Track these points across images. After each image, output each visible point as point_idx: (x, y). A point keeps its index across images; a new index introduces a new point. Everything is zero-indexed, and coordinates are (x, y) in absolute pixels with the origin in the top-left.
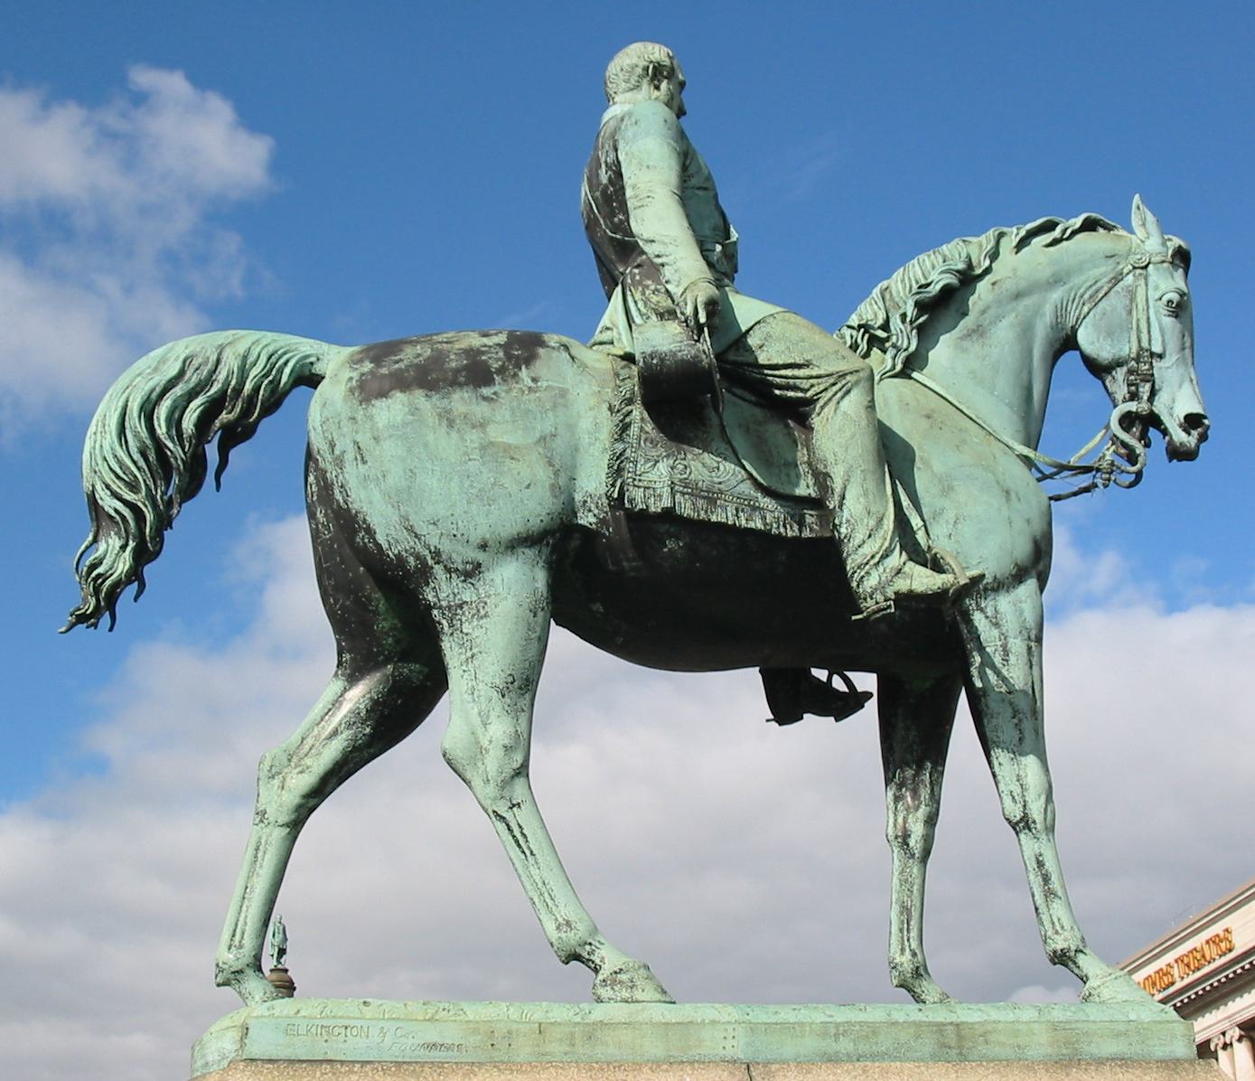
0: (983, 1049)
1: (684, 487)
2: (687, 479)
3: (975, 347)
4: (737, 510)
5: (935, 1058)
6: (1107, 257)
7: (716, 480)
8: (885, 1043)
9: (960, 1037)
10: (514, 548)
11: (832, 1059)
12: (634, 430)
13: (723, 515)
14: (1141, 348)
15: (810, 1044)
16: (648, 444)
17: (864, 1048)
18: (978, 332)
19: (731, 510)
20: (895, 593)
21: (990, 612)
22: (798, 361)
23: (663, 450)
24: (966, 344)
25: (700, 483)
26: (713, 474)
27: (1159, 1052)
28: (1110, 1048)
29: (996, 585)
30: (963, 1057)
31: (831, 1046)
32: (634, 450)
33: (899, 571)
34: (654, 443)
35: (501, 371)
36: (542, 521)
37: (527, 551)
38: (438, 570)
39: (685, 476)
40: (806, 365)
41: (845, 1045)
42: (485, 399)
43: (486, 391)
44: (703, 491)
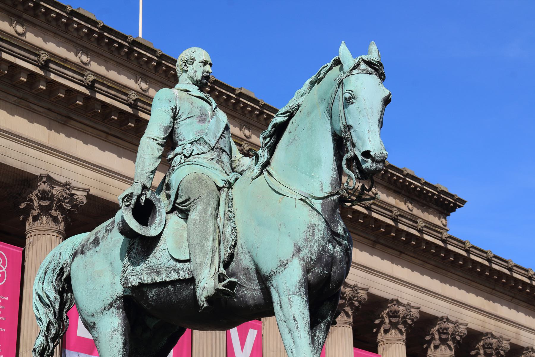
1: (148, 270)
2: (149, 267)
4: (168, 274)
6: (334, 80)
7: (159, 263)
10: (102, 313)
12: (134, 250)
13: (165, 277)
14: (344, 126)
16: (138, 255)
20: (205, 298)
21: (274, 285)
23: (142, 256)
25: (153, 267)
26: (159, 261)
29: (273, 273)
32: (132, 260)
34: (139, 254)
36: (108, 299)
37: (107, 312)
39: (148, 266)
43: (97, 249)
44: (154, 270)
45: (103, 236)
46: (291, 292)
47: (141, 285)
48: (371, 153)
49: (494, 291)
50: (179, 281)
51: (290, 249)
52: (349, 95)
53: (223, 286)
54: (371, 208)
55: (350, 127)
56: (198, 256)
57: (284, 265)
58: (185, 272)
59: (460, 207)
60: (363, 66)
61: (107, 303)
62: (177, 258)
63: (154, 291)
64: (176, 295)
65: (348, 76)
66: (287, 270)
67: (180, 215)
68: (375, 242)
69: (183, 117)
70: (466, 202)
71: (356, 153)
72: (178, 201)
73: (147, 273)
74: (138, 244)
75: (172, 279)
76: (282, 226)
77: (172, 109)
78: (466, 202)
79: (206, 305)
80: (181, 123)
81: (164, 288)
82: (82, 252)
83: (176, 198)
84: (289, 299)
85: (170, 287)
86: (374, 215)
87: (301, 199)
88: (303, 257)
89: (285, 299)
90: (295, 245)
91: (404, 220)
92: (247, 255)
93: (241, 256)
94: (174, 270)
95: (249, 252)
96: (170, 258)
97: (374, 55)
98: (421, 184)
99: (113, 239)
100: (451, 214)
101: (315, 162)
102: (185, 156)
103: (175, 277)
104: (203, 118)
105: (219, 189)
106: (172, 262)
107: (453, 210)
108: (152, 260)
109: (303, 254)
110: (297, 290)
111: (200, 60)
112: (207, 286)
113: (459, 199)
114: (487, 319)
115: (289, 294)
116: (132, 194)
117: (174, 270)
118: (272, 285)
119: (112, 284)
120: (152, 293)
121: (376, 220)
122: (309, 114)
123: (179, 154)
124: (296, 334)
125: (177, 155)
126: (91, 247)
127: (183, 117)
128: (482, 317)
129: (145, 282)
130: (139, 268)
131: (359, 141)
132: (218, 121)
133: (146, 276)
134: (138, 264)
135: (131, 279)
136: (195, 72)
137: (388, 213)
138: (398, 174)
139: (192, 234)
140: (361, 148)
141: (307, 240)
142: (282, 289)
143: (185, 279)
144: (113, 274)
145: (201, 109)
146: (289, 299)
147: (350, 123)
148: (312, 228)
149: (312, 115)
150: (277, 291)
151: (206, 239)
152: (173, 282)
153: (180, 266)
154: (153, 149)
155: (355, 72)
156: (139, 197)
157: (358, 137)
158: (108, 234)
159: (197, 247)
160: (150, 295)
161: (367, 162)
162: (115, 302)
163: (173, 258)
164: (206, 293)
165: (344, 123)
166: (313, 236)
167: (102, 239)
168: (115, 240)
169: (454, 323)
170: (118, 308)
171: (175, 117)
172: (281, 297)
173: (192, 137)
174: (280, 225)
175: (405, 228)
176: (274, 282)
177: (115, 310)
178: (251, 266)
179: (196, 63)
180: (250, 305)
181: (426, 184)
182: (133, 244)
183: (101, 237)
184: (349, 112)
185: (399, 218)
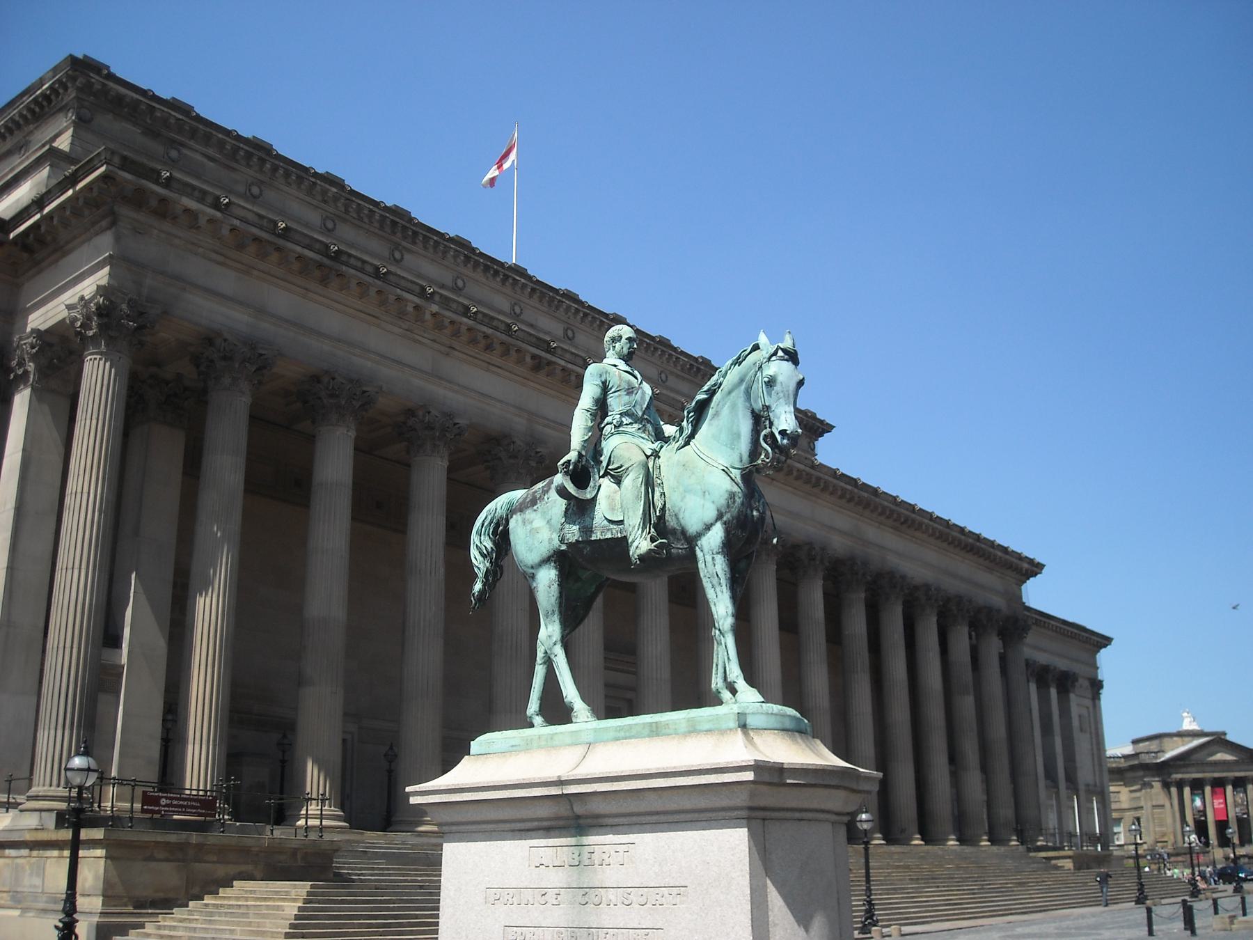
0: (664, 731)
3: (715, 422)
5: (649, 736)
8: (634, 732)
9: (657, 727)
11: (617, 739)
12: (571, 510)
15: (612, 734)
17: (628, 734)
18: (717, 414)
19: (599, 534)
21: (699, 545)
24: (712, 422)
30: (658, 735)
40: (621, 466)
41: (622, 734)
42: (535, 510)
43: (535, 508)
45: (540, 497)
46: (714, 552)
48: (788, 432)
57: (708, 527)
60: (780, 353)
62: (610, 519)
67: (612, 480)
69: (613, 390)
70: (834, 427)
71: (774, 431)
72: (610, 467)
74: (574, 506)
75: (606, 537)
76: (707, 493)
77: (603, 383)
78: (834, 427)
80: (611, 395)
83: (608, 465)
84: (713, 558)
87: (723, 470)
89: (709, 558)
90: (718, 510)
94: (608, 530)
96: (604, 518)
97: (787, 343)
99: (550, 499)
100: (820, 439)
104: (630, 391)
105: (648, 457)
107: (821, 435)
109: (725, 519)
110: (720, 550)
111: (627, 337)
115: (713, 554)
117: (608, 530)
119: (550, 540)
123: (610, 424)
124: (718, 589)
125: (607, 424)
127: (613, 390)
132: (644, 393)
135: (568, 536)
136: (622, 348)
141: (728, 506)
142: (706, 549)
143: (618, 538)
145: (629, 383)
146: (713, 558)
148: (732, 495)
150: (702, 551)
153: (612, 526)
154: (586, 420)
155: (774, 358)
156: (576, 464)
162: (553, 556)
163: (606, 518)
164: (638, 552)
166: (734, 502)
167: (539, 498)
171: (605, 387)
173: (622, 409)
174: (704, 492)
177: (552, 564)
179: (623, 340)
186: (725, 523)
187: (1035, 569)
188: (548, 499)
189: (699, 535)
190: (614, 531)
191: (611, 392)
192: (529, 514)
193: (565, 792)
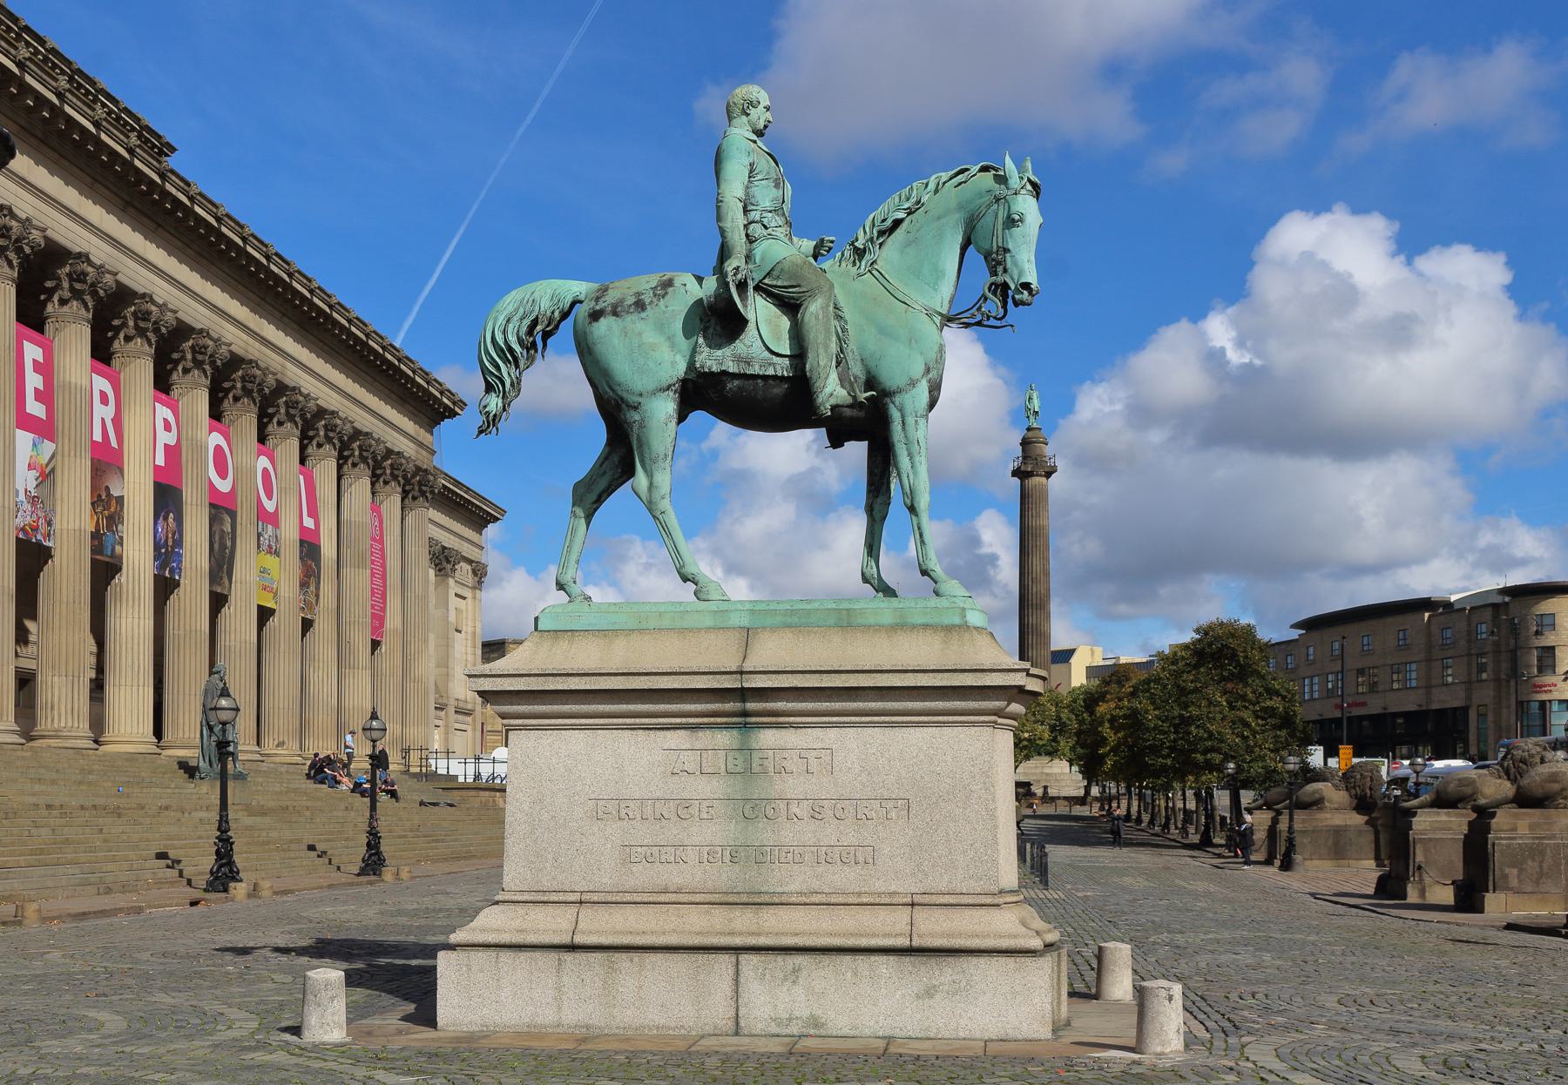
9: (848, 615)
13: (756, 369)
14: (998, 246)
19: (757, 367)
22: (794, 284)
27: (947, 621)
28: (919, 620)
31: (789, 620)
33: (832, 395)
34: (720, 336)
35: (651, 302)
38: (624, 406)
43: (643, 315)
46: (919, 415)
47: (724, 373)
49: (263, 303)
50: (775, 377)
51: (921, 368)
52: (1018, 217)
53: (865, 399)
54: (134, 151)
55: (1006, 250)
56: (821, 357)
57: (913, 383)
58: (782, 368)
59: (167, 155)
60: (1029, 187)
61: (665, 384)
62: (773, 349)
63: (736, 383)
64: (764, 392)
65: (1016, 194)
66: (915, 390)
68: (127, 202)
69: (759, 177)
70: (176, 150)
72: (766, 281)
73: (733, 361)
74: (716, 324)
76: (913, 341)
77: (750, 165)
78: (176, 150)
79: (829, 414)
81: (751, 382)
82: (615, 314)
84: (916, 421)
85: (759, 381)
86: (137, 163)
88: (930, 379)
89: (910, 420)
90: (926, 364)
91: (173, 178)
92: (859, 364)
93: (851, 363)
94: (770, 364)
95: (862, 360)
98: (119, 109)
99: (670, 308)
101: (938, 274)
102: (766, 227)
103: (770, 372)
106: (767, 354)
108: (739, 346)
109: (930, 376)
112: (835, 393)
113: (168, 143)
114: (251, 341)
116: (738, 267)
117: (770, 364)
118: (893, 403)
120: (732, 385)
121: (138, 170)
122: (939, 218)
124: (917, 459)
126: (632, 310)
127: (759, 177)
128: (245, 337)
129: (731, 370)
130: (719, 353)
131: (1015, 269)
133: (731, 364)
134: (719, 347)
137: (155, 163)
138: (87, 86)
139: (814, 330)
140: (1016, 277)
141: (937, 361)
142: (909, 408)
143: (783, 376)
144: (673, 351)
146: (916, 421)
147: (1010, 247)
149: (943, 221)
151: (830, 340)
152: (765, 378)
157: (1015, 264)
158: (659, 300)
159: (821, 346)
160: (729, 386)
161: (1022, 293)
162: (674, 385)
163: (768, 349)
164: (833, 401)
165: (1000, 244)
168: (673, 311)
169: (215, 341)
170: (675, 392)
172: (906, 418)
174: (911, 340)
175: (174, 191)
176: (897, 399)
177: (671, 394)
178: (861, 376)
180: (845, 416)
181: (126, 111)
182: (709, 321)
183: (647, 301)
184: (1011, 236)
185: (169, 174)
186: (929, 381)
187: (457, 409)
188: (666, 307)
189: (900, 391)
190: (778, 368)
191: (756, 179)
192: (633, 321)
193: (746, 685)
